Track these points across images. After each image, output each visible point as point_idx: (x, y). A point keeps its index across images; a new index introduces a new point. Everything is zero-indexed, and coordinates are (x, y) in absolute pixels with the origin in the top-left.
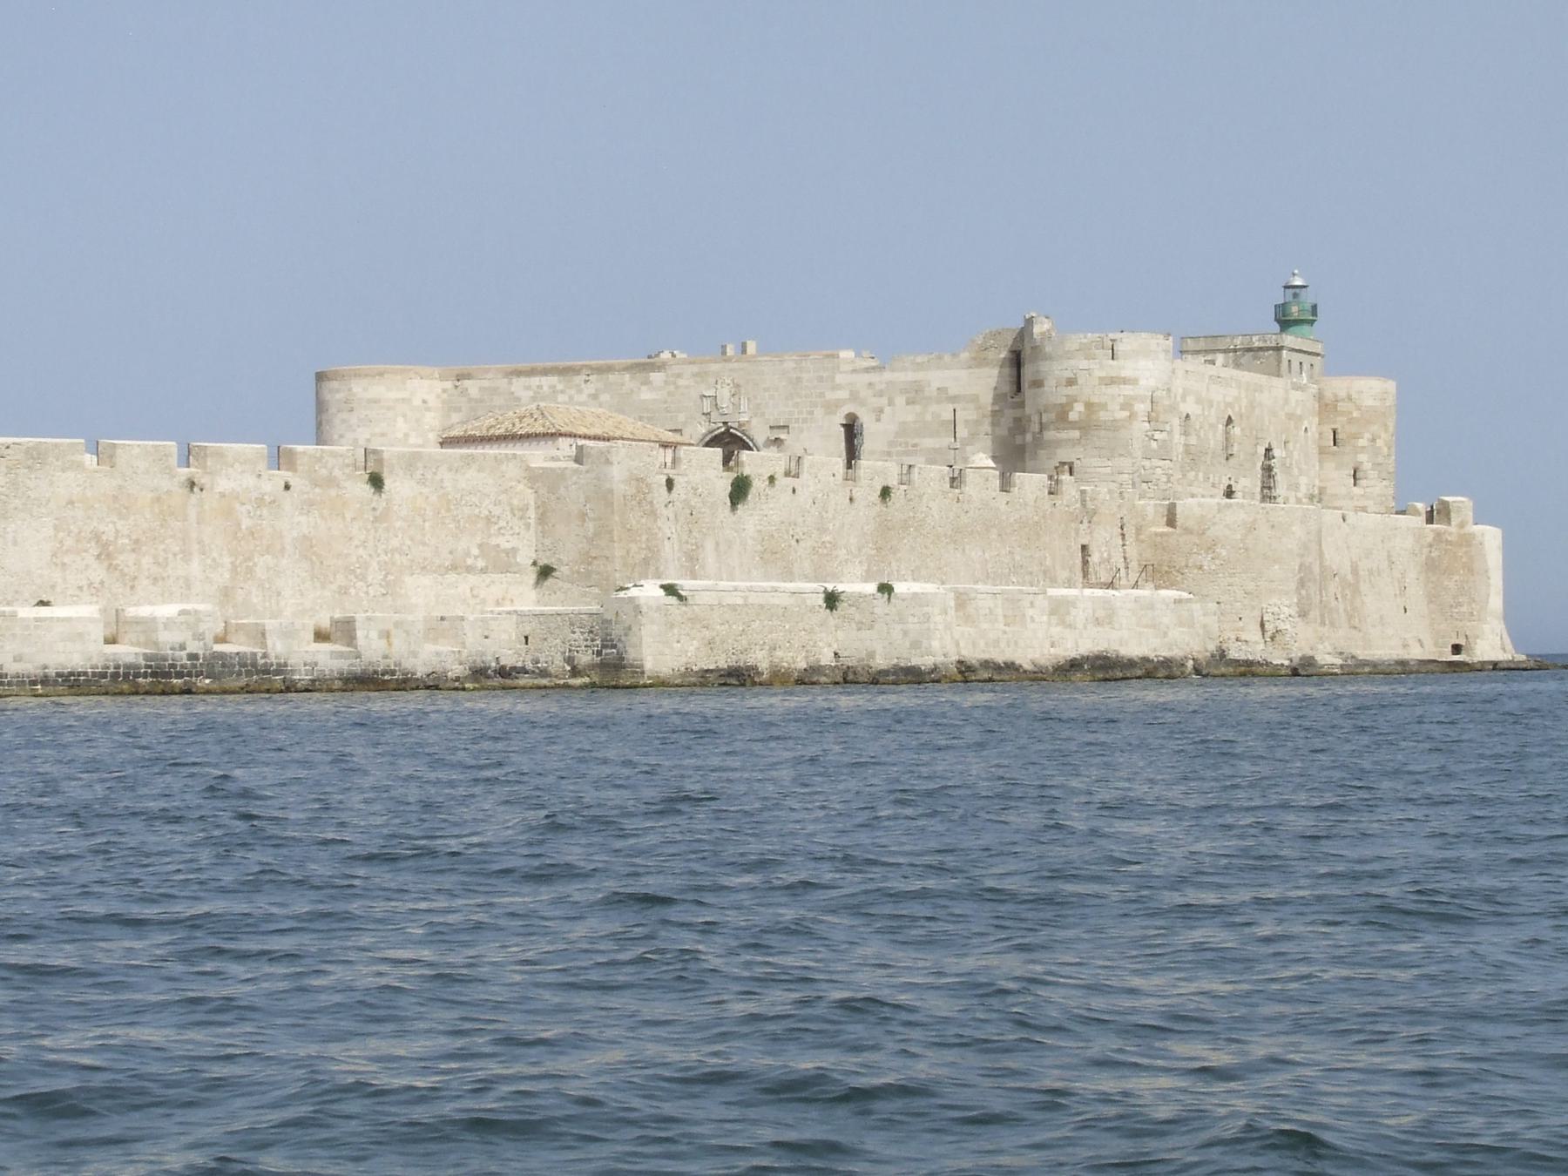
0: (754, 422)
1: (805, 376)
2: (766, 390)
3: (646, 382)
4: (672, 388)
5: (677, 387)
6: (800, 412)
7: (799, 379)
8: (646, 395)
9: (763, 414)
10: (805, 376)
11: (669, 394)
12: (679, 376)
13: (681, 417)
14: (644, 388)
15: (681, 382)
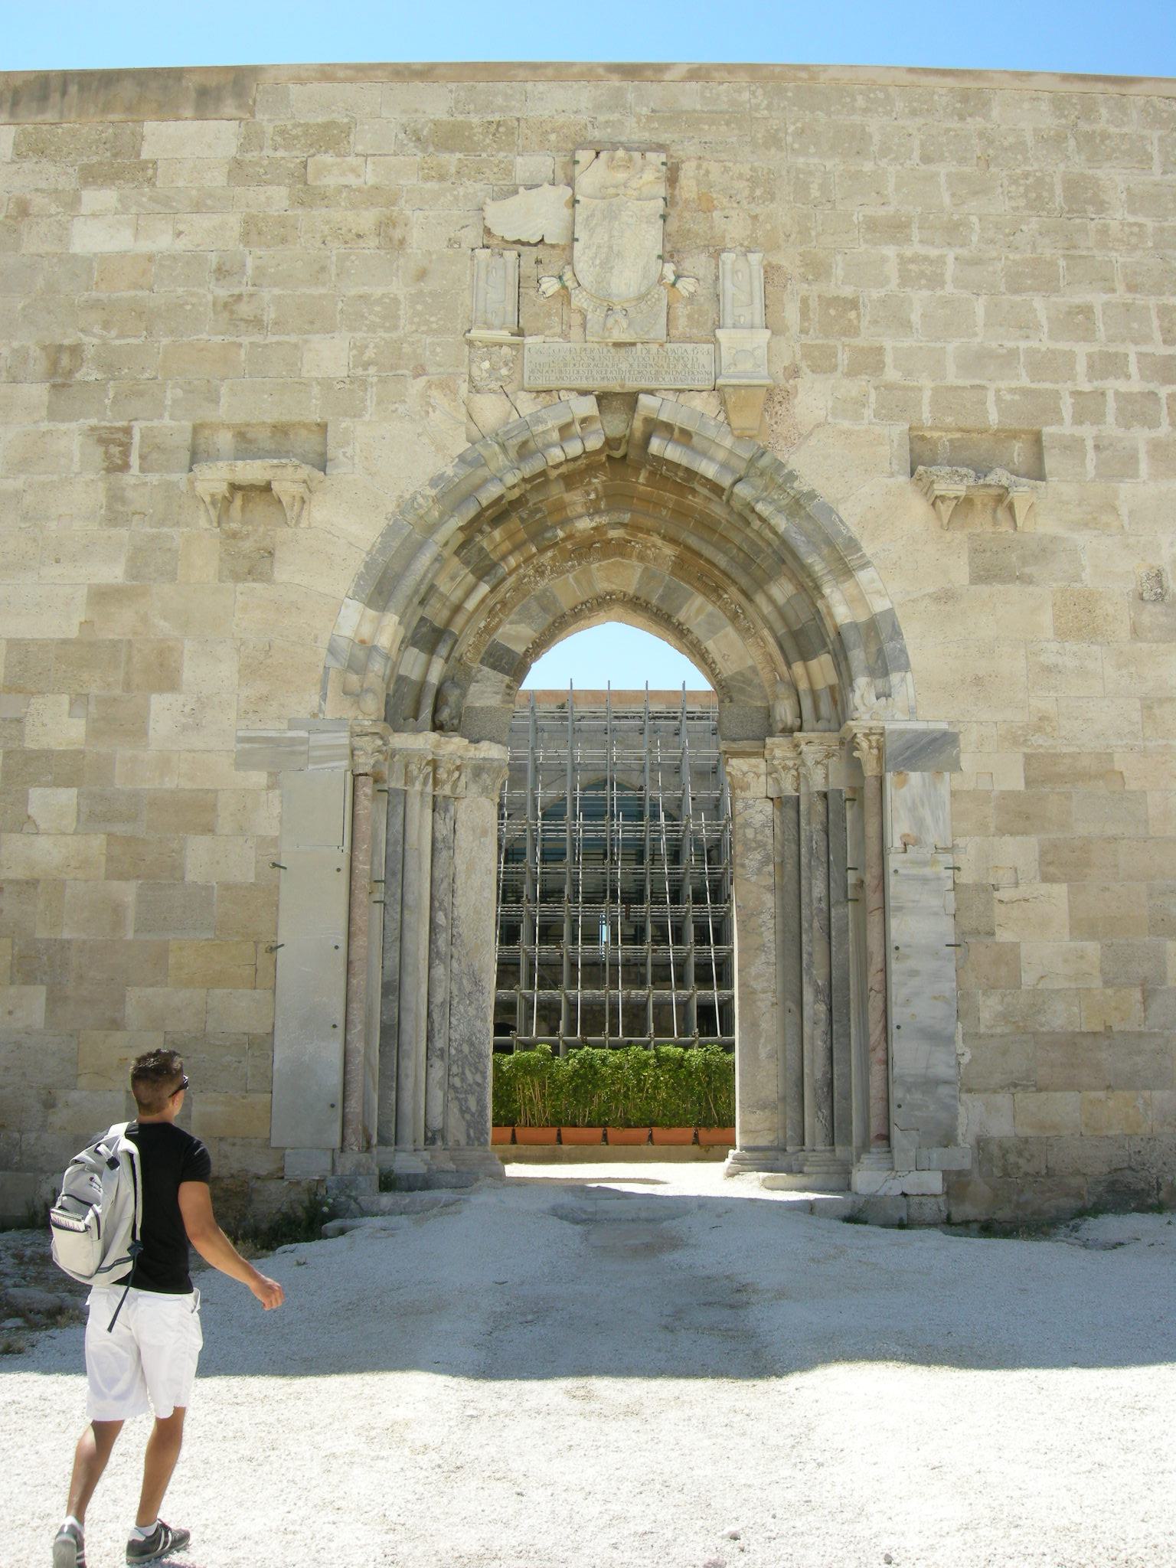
0: (812, 399)
1: (1115, 178)
2: (895, 229)
3: (122, 167)
4: (278, 197)
5: (307, 194)
6: (1108, 364)
7: (1082, 196)
8: (102, 229)
9: (870, 362)
10: (1115, 178)
11: (252, 230)
12: (331, 137)
13: (328, 356)
14: (99, 198)
15: (332, 171)
